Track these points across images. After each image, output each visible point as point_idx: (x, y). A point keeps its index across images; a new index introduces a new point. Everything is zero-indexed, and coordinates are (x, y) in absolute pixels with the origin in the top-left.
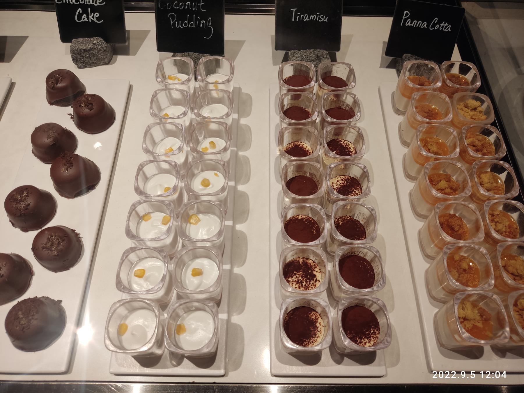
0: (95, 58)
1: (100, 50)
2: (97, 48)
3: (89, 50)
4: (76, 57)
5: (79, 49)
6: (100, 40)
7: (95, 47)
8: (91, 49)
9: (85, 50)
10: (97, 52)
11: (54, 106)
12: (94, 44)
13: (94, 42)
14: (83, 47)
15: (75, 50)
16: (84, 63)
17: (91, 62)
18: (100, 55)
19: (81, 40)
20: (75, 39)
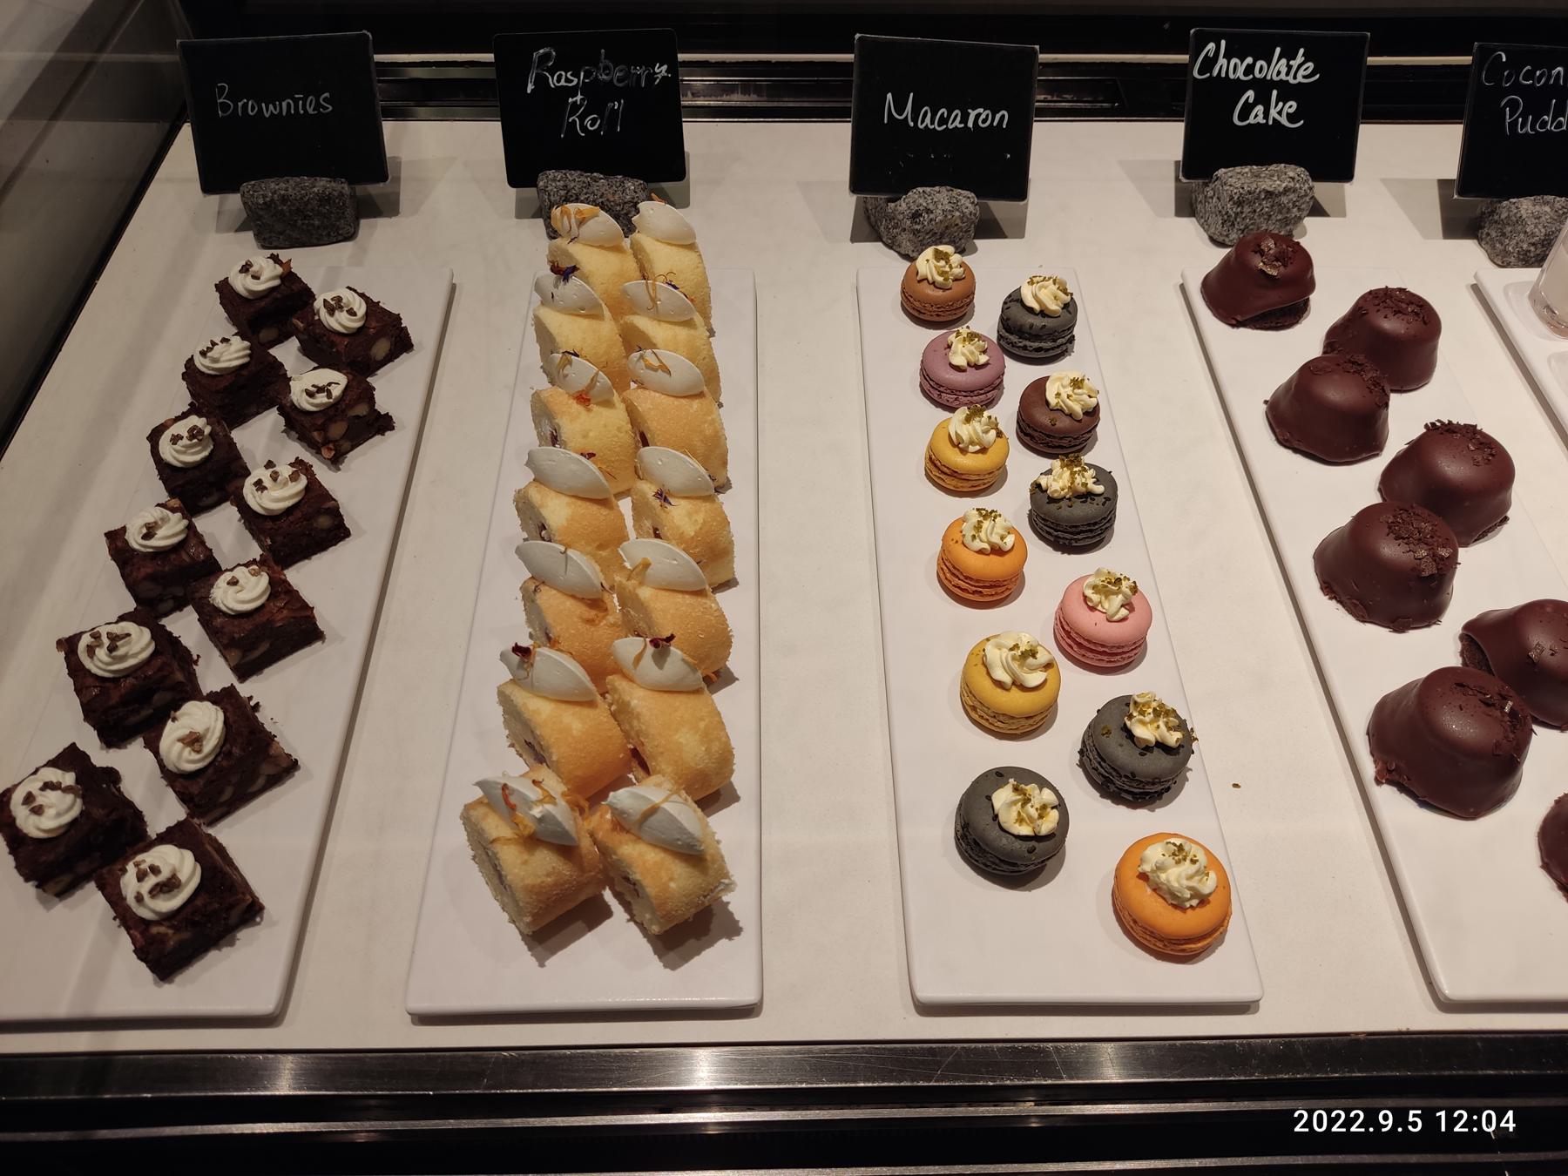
0: (1279, 217)
1: (1306, 195)
2: (1301, 188)
3: (1280, 194)
4: (1237, 214)
5: (1258, 191)
6: (1300, 170)
7: (1297, 186)
8: (1286, 191)
9: (1269, 194)
10: (1294, 199)
11: (1242, 330)
12: (1293, 179)
13: (1291, 174)
14: (1267, 185)
15: (1249, 192)
16: (1242, 233)
17: (1264, 227)
18: (1295, 210)
19: (1247, 170)
20: (1224, 170)
